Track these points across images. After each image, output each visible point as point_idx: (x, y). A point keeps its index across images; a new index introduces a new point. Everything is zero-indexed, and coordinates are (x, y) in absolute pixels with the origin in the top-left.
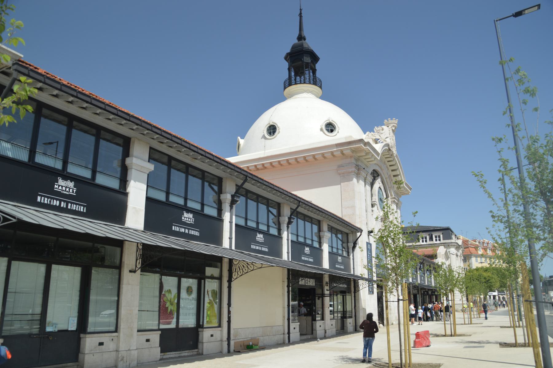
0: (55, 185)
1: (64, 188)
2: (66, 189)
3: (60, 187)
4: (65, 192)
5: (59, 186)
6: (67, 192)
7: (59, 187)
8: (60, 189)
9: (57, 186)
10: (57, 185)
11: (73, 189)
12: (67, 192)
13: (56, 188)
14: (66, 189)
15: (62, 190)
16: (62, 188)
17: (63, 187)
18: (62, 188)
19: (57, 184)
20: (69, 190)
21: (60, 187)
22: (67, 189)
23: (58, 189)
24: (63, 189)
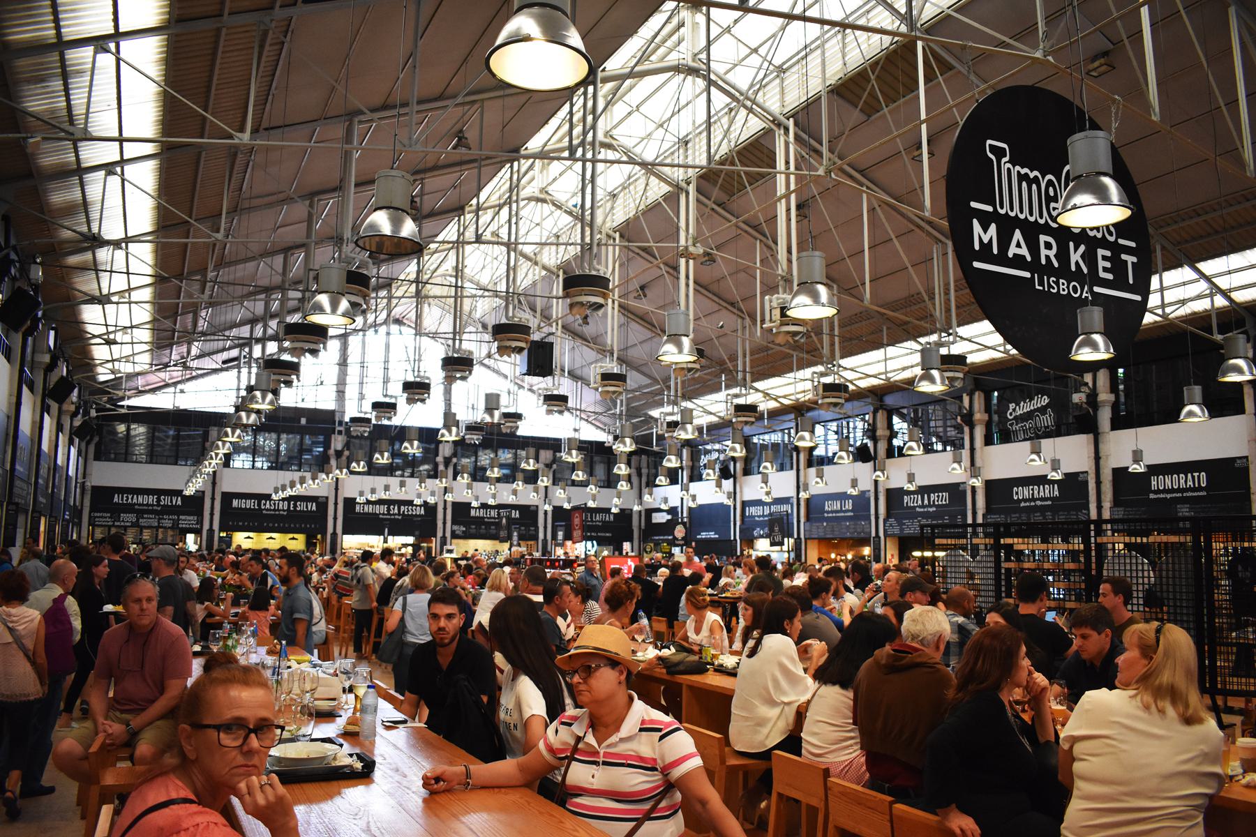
0: (977, 227)
1: (1048, 254)
2: (1063, 255)
3: (1018, 235)
4: (1064, 287)
5: (1007, 226)
6: (1078, 276)
7: (1005, 241)
8: (1018, 262)
9: (993, 229)
10: (985, 221)
11: (1116, 249)
12: (1078, 276)
13: (985, 253)
14: (1063, 255)
15: (1034, 266)
16: (1034, 248)
17: (1043, 238)
18: (1034, 248)
19: (989, 209)
20: (1090, 257)
21: (1018, 235)
22: (1075, 257)
23: (1002, 259)
24: (1044, 252)
